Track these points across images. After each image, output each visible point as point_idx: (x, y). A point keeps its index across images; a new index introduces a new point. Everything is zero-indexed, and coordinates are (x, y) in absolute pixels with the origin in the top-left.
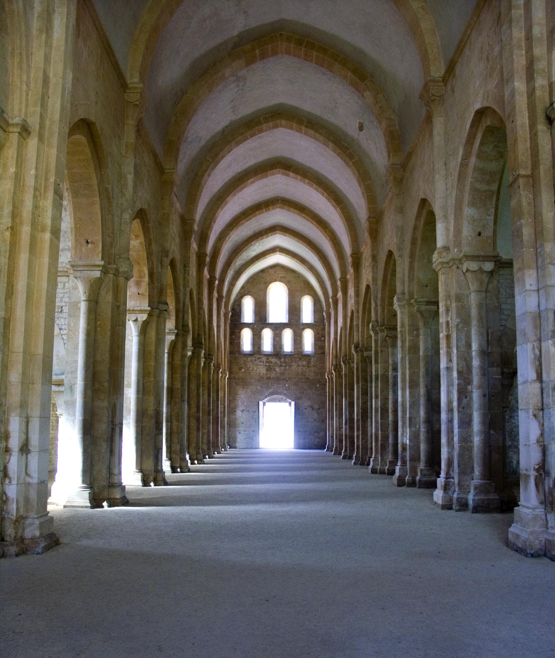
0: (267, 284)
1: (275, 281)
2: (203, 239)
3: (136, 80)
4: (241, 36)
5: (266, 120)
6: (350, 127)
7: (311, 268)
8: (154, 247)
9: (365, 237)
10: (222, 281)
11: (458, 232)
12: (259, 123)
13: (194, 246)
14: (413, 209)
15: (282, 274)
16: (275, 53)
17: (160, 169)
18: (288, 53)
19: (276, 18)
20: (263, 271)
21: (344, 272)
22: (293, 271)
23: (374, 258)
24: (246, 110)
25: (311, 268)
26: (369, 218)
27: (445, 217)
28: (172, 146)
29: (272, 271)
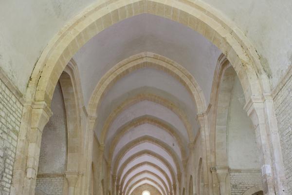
0: (142, 192)
1: (145, 190)
2: (119, 180)
3: (103, 143)
4: (133, 120)
5: (141, 140)
6: (171, 145)
7: (159, 186)
8: (105, 190)
9: (177, 180)
10: (124, 192)
11: (199, 189)
12: (139, 141)
13: (116, 183)
14: (190, 176)
15: (148, 187)
16: (144, 123)
17: (107, 163)
18: (148, 123)
19: (144, 114)
20: (140, 186)
21: (171, 190)
22: (152, 186)
23: (180, 189)
24: (134, 138)
25: (159, 186)
26: (178, 174)
27: (196, 184)
28: (110, 155)
29: (143, 186)
